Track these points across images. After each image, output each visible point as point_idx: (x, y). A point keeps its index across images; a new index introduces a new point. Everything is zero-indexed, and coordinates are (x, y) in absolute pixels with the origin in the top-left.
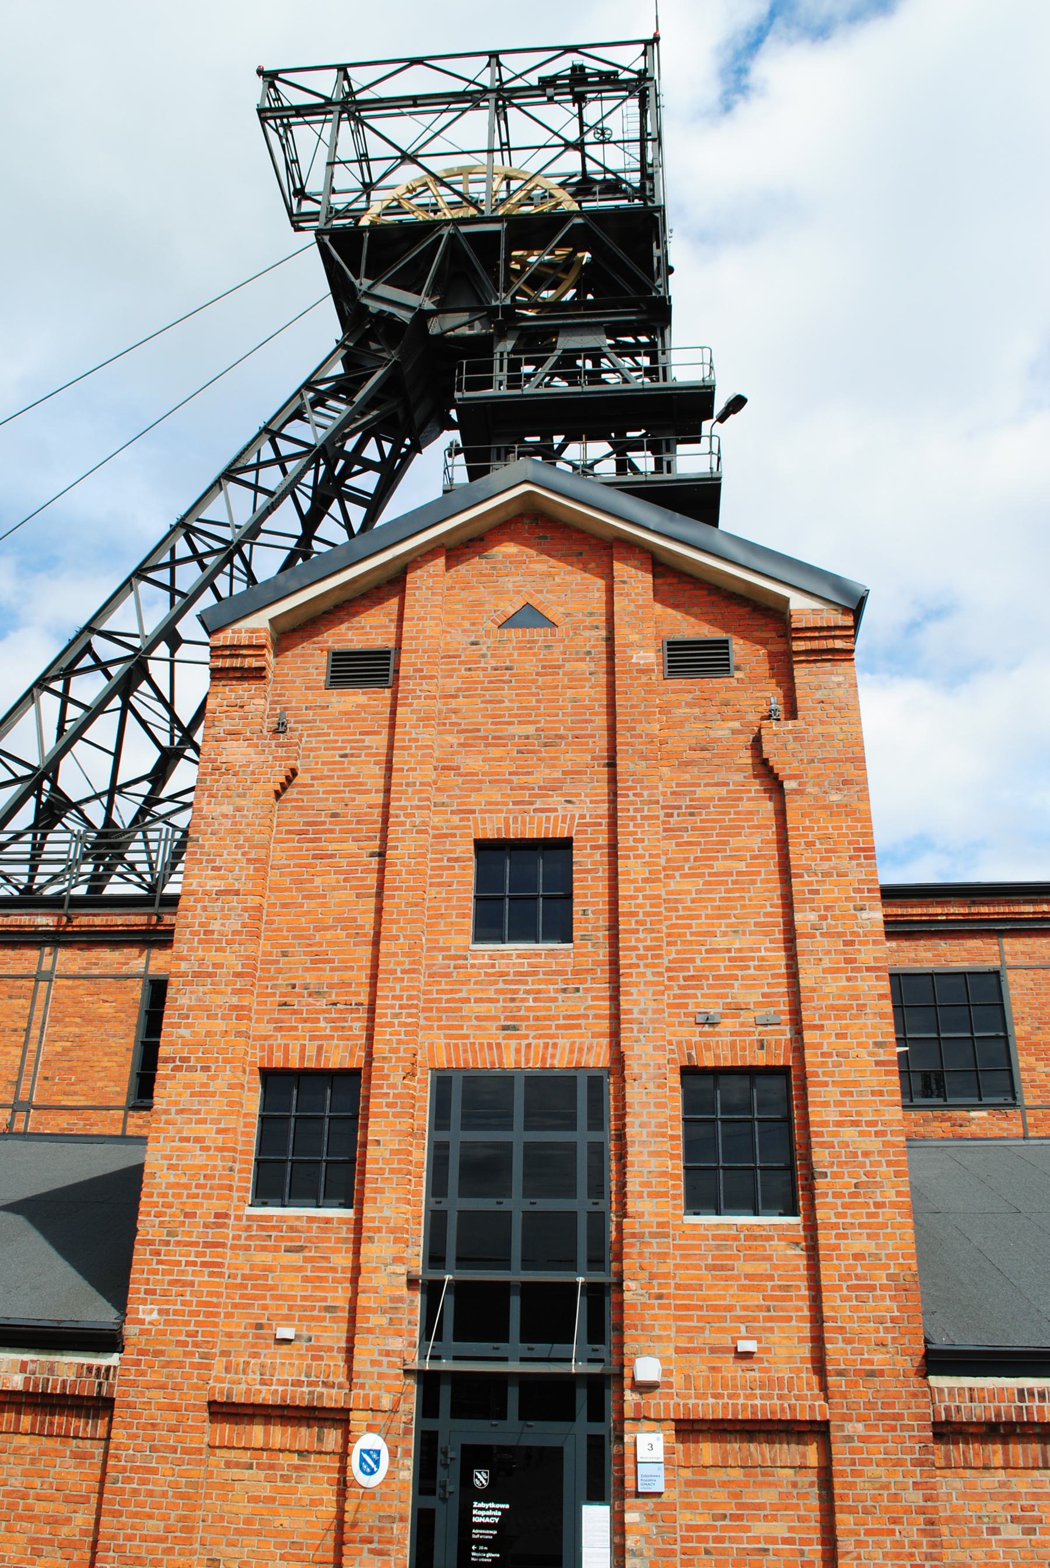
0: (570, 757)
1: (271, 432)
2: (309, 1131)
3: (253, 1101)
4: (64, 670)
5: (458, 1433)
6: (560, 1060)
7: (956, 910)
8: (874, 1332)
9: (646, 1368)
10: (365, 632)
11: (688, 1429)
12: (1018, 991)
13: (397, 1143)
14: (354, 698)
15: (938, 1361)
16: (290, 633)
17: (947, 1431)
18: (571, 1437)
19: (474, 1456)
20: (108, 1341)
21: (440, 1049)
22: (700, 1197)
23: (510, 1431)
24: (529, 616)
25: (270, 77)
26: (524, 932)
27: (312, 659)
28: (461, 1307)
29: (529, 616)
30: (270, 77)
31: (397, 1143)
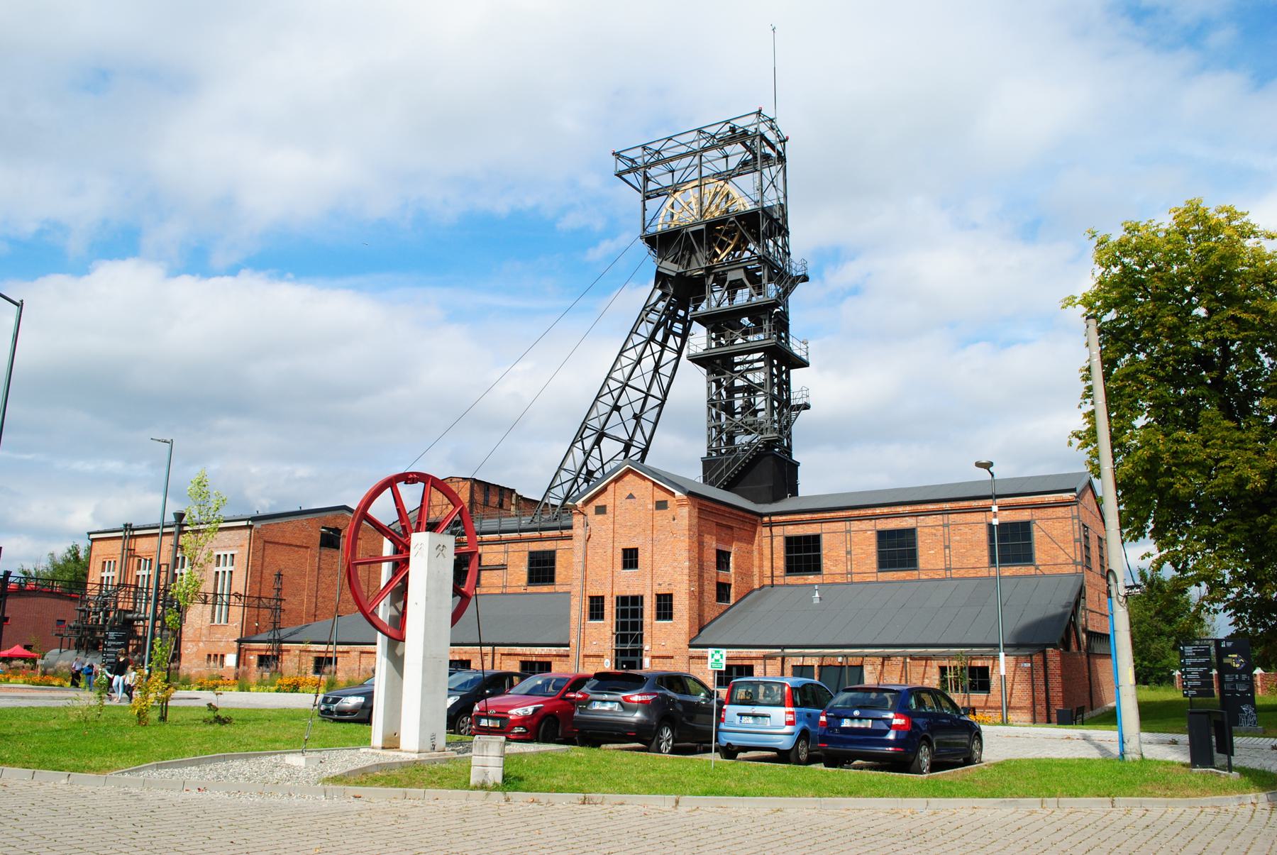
0: (638, 530)
1: (634, 331)
2: (596, 608)
3: (588, 602)
4: (579, 437)
5: (621, 659)
6: (636, 594)
7: (808, 516)
8: (683, 640)
9: (646, 647)
10: (599, 502)
11: (653, 657)
12: (825, 541)
13: (610, 608)
14: (600, 517)
15: (690, 646)
16: (586, 503)
17: (692, 657)
18: (637, 659)
19: (623, 663)
20: (568, 645)
21: (617, 592)
22: (659, 617)
23: (629, 658)
24: (631, 496)
25: (617, 155)
26: (631, 567)
27: (590, 510)
28: (621, 639)
29: (631, 496)
30: (617, 155)
31: (610, 608)
